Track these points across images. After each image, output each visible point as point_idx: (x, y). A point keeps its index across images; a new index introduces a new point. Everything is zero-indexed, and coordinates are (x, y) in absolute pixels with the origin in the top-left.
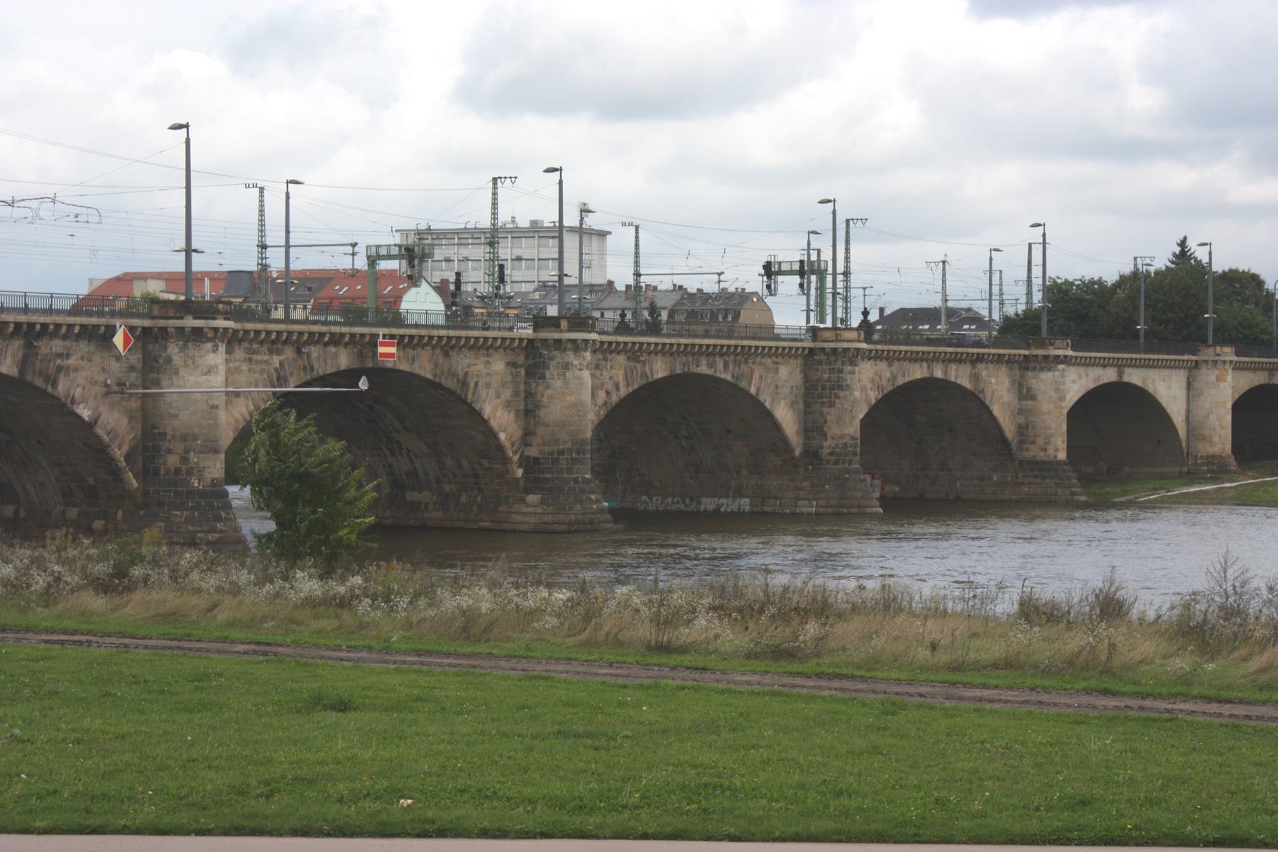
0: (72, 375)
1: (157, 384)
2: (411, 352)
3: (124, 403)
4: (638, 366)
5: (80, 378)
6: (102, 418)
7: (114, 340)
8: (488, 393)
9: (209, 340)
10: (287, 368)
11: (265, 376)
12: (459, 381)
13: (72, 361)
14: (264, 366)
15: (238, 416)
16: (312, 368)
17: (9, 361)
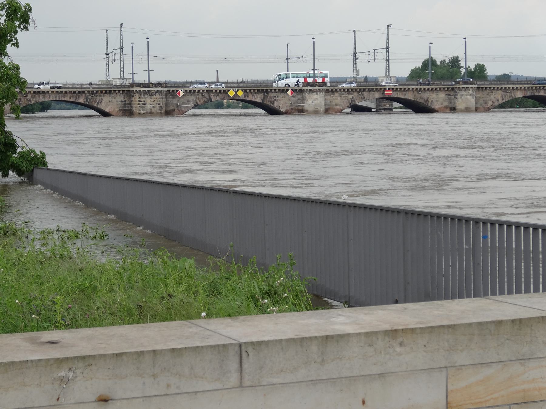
1: (304, 103)
2: (404, 93)
4: (508, 94)
5: (282, 102)
8: (437, 103)
9: (315, 92)
10: (355, 98)
11: (347, 100)
12: (424, 100)
14: (346, 98)
17: (259, 98)
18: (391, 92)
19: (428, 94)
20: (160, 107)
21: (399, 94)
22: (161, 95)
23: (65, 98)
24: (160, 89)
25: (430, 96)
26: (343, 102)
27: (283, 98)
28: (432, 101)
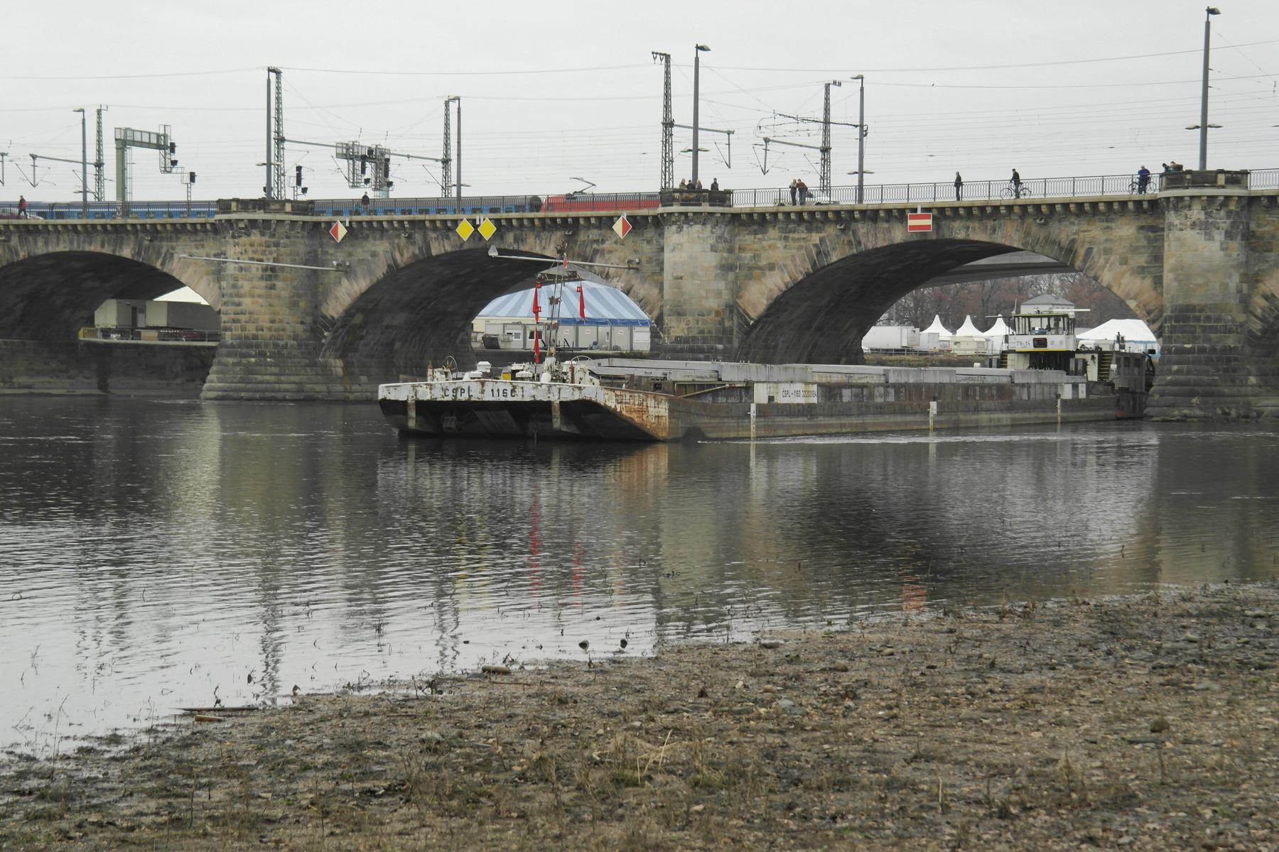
0: (607, 256)
2: (990, 223)
3: (655, 278)
5: (614, 258)
6: (634, 289)
7: (614, 227)
9: (674, 223)
11: (803, 251)
12: (1061, 248)
13: (607, 245)
14: (802, 243)
15: (773, 287)
16: (859, 243)
18: (929, 222)
19: (1075, 228)
20: (265, 269)
21: (974, 229)
22: (273, 236)
23: (58, 244)
24: (260, 215)
25: (1082, 235)
26: (793, 259)
27: (618, 246)
28: (1089, 251)
